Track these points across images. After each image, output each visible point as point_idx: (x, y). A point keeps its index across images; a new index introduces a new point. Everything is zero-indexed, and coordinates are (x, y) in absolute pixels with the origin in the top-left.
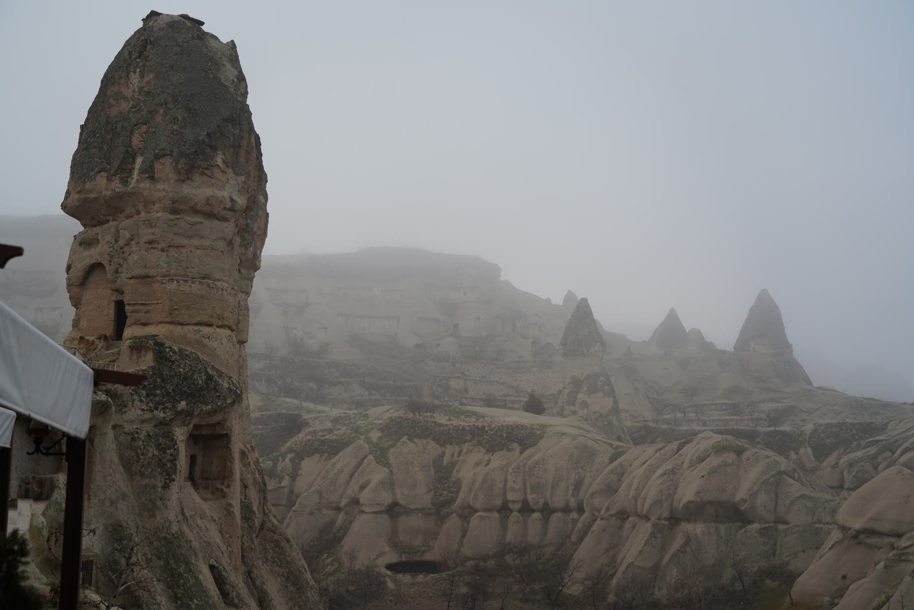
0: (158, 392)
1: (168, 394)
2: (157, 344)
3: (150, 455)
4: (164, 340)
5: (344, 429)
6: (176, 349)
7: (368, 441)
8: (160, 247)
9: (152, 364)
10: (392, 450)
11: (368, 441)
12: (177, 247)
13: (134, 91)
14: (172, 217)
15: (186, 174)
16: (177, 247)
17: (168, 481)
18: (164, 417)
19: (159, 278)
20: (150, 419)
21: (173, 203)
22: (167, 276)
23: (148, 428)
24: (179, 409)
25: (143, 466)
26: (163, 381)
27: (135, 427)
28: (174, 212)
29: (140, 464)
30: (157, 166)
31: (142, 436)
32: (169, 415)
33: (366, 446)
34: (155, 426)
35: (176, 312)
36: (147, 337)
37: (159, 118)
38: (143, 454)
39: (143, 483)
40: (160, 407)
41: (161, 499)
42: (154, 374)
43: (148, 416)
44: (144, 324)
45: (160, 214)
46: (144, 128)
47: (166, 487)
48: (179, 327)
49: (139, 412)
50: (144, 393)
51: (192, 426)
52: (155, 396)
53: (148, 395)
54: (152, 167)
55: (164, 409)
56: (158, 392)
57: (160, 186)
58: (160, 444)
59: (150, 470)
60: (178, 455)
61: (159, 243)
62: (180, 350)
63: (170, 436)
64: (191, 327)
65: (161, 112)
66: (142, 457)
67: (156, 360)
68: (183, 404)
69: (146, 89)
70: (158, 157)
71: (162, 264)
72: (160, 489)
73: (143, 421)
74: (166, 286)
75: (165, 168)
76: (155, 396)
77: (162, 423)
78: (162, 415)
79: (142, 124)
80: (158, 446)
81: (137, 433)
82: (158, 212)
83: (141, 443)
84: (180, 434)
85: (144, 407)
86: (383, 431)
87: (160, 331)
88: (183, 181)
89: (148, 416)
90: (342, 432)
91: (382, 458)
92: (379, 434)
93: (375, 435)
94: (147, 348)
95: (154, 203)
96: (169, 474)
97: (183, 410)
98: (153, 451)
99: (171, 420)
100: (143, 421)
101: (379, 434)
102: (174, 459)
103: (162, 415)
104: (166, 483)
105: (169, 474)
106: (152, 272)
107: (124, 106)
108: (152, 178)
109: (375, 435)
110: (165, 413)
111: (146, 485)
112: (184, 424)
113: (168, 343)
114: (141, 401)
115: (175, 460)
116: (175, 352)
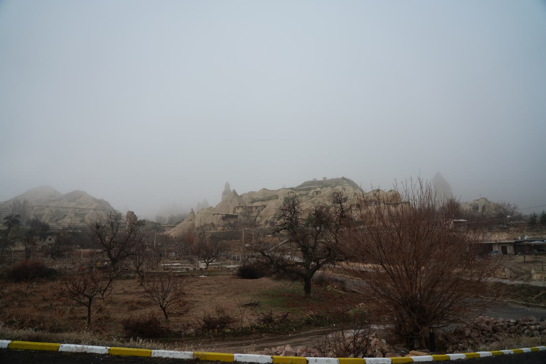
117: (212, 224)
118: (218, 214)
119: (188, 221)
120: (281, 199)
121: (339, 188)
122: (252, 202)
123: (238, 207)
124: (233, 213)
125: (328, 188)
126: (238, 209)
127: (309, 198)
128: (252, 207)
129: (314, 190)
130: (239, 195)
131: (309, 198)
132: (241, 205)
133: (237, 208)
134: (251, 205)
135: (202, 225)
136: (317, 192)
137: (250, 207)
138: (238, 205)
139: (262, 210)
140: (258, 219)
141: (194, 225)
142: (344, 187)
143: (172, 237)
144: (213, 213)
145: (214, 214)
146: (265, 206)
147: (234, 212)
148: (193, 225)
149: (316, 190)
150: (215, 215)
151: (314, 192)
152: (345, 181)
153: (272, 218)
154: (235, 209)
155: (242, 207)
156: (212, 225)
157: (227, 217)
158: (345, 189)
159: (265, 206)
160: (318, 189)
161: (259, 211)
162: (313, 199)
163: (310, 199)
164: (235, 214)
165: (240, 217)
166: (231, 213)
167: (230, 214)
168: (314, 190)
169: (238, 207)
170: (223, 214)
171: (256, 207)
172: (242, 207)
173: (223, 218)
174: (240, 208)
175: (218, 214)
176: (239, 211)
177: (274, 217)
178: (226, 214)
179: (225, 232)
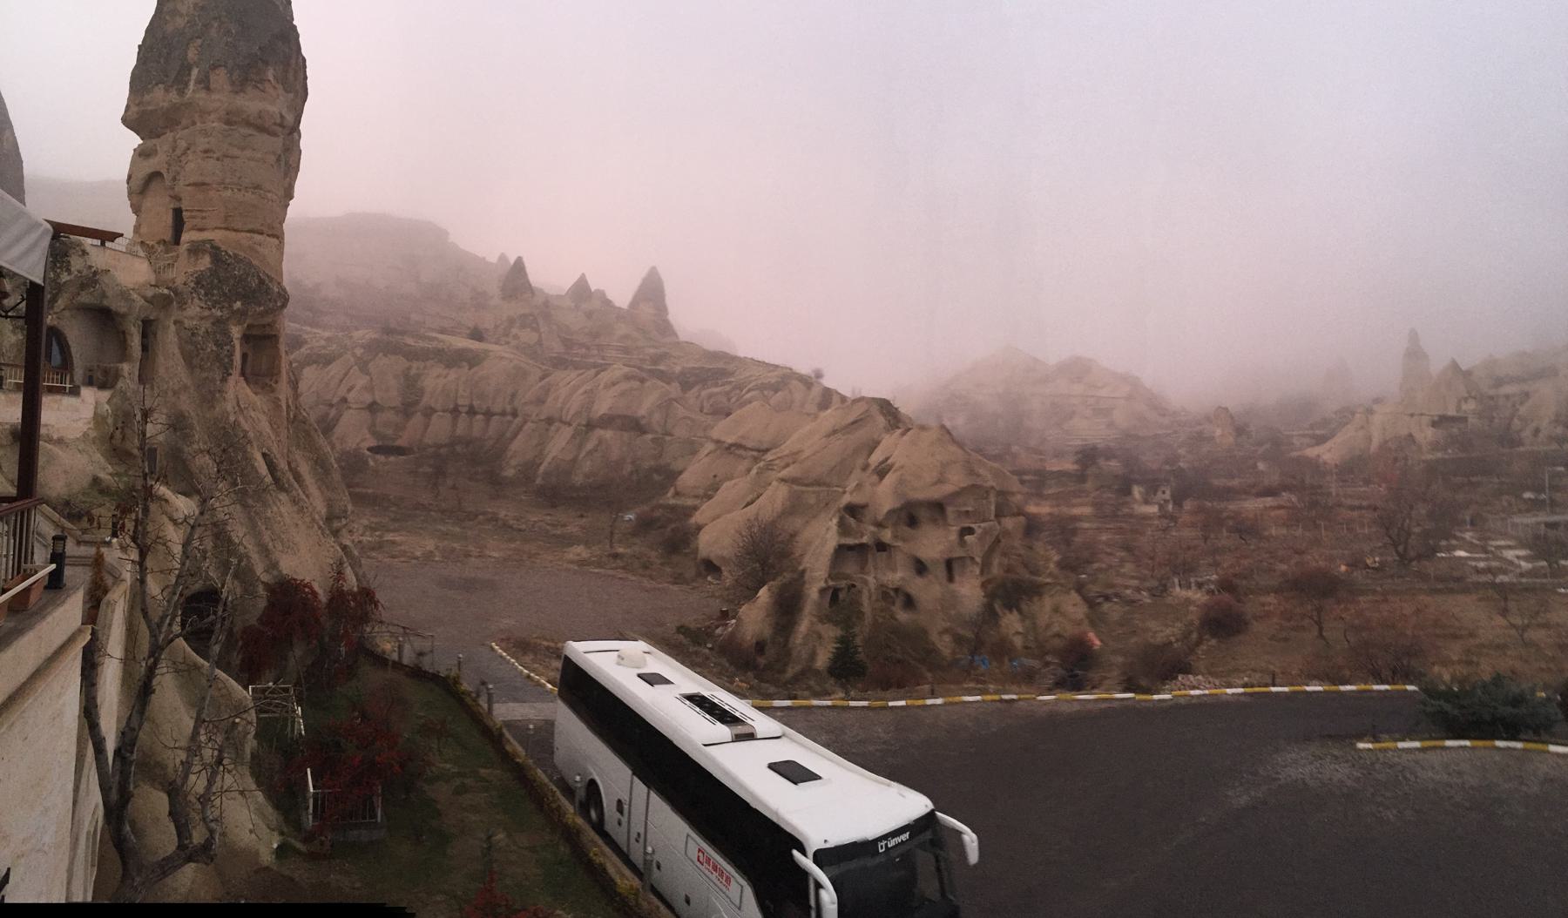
0: (215, 292)
1: (225, 294)
2: (212, 247)
3: (209, 350)
4: (220, 245)
5: (334, 347)
6: (231, 253)
7: (354, 355)
8: (215, 156)
9: (209, 266)
10: (372, 363)
11: (354, 355)
12: (232, 157)
13: (189, 8)
14: (226, 127)
15: (240, 86)
16: (232, 157)
17: (225, 375)
18: (221, 316)
19: (214, 186)
20: (209, 316)
21: (228, 114)
22: (223, 183)
23: (207, 325)
24: (235, 309)
25: (202, 359)
26: (220, 282)
27: (194, 323)
28: (228, 123)
29: (199, 358)
30: (213, 77)
31: (201, 333)
32: (226, 313)
33: (352, 359)
34: (213, 324)
35: (230, 219)
36: (204, 242)
37: (213, 32)
38: (202, 349)
39: (205, 375)
40: (218, 306)
41: (219, 391)
42: (211, 275)
43: (206, 313)
44: (201, 230)
45: (214, 125)
46: (199, 41)
47: (224, 380)
48: (234, 233)
49: (198, 309)
50: (203, 292)
51: (246, 325)
52: (213, 295)
53: (206, 294)
54: (207, 77)
55: (221, 309)
56: (215, 292)
57: (215, 96)
58: (218, 341)
59: (209, 364)
60: (234, 351)
61: (214, 153)
62: (235, 254)
63: (226, 333)
64: (243, 234)
65: (216, 25)
66: (201, 352)
67: (212, 262)
68: (238, 305)
69: (200, 5)
70: (214, 67)
71: (217, 172)
72: (218, 382)
73: (202, 318)
74: (221, 193)
75: (220, 78)
76: (213, 295)
77: (218, 322)
78: (219, 313)
79: (197, 38)
80: (217, 343)
81: (196, 329)
82: (213, 122)
83: (200, 338)
84: (236, 332)
85: (203, 305)
86: (365, 348)
87: (216, 236)
88: (237, 93)
89: (206, 313)
90: (333, 348)
91: (364, 369)
92: (362, 351)
93: (359, 352)
94: (204, 252)
95: (209, 113)
96: (226, 368)
97: (238, 309)
98: (211, 347)
99: (228, 319)
100: (202, 318)
101: (362, 351)
102: (231, 355)
103: (219, 313)
104: (223, 377)
105: (226, 368)
106: (208, 180)
107: (180, 22)
108: (208, 89)
109: (359, 352)
110: (221, 311)
111: (207, 378)
112: (239, 323)
113: (223, 248)
114: (200, 299)
115: (232, 355)
116: (230, 256)
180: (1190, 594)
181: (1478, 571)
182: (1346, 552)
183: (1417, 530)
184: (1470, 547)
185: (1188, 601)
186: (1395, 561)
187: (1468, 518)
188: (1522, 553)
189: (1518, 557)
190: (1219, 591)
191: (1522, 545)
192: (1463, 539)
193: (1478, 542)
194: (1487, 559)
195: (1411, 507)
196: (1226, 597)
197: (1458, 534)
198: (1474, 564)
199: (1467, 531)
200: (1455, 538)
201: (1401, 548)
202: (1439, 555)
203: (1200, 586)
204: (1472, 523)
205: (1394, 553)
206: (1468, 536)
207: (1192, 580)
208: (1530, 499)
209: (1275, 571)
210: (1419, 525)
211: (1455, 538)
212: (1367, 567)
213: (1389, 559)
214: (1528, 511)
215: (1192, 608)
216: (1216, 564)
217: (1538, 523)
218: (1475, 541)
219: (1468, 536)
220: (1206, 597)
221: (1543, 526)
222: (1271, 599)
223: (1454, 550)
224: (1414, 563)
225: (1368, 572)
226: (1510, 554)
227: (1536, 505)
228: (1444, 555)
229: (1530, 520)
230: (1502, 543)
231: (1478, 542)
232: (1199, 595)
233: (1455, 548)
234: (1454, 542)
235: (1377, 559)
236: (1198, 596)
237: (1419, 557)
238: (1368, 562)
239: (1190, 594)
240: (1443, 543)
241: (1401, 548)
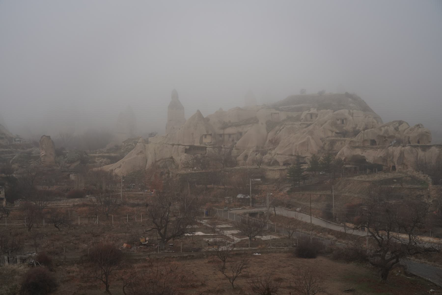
117: (172, 158)
118: (179, 145)
119: (138, 154)
120: (262, 124)
121: (345, 112)
122: (224, 128)
123: (206, 136)
124: (200, 144)
125: (328, 110)
126: (205, 137)
127: (304, 126)
128: (224, 134)
129: (307, 112)
130: (205, 117)
131: (304, 126)
132: (210, 133)
133: (204, 137)
134: (221, 132)
135: (157, 160)
136: (311, 115)
137: (221, 135)
138: (206, 133)
139: (238, 139)
140: (235, 151)
141: (147, 160)
142: (351, 111)
143: (116, 175)
144: (171, 143)
145: (173, 145)
146: (241, 134)
147: (201, 142)
148: (146, 159)
149: (310, 112)
150: (175, 146)
151: (308, 114)
152: (350, 99)
153: (253, 151)
154: (201, 138)
155: (211, 135)
156: (172, 160)
157: (190, 150)
158: (353, 113)
159: (241, 134)
160: (313, 111)
161: (233, 140)
162: (311, 127)
163: (306, 127)
164: (202, 145)
165: (209, 149)
166: (197, 144)
167: (196, 145)
168: (307, 112)
169: (206, 136)
170: (186, 144)
171: (230, 135)
172: (211, 135)
173: (186, 151)
174: (208, 137)
175: (179, 145)
176: (207, 140)
177: (256, 151)
178: (191, 144)
179: (198, 173)
180: (15, 267)
181: (209, 244)
182: (127, 234)
183: (174, 219)
184: (205, 229)
185: (14, 272)
186: (158, 239)
187: (205, 211)
188: (235, 232)
189: (233, 235)
190: (37, 264)
191: (235, 228)
192: (201, 224)
193: (210, 226)
194: (213, 237)
195: (170, 205)
196: (43, 267)
197: (198, 221)
198: (207, 240)
199: (204, 219)
200: (197, 223)
201: (162, 231)
202: (186, 235)
203: (23, 261)
204: (207, 215)
205: (159, 235)
206: (204, 222)
207: (18, 257)
208: (241, 198)
209: (78, 249)
210: (174, 216)
211: (197, 223)
212: (141, 244)
213: (155, 238)
214: (240, 206)
215: (16, 277)
216: (36, 246)
217: (245, 214)
218: (209, 226)
219: (204, 222)
220: (28, 269)
221: (247, 215)
222: (75, 268)
223: (195, 232)
224: (171, 240)
225: (141, 248)
226: (228, 233)
227: (243, 203)
228: (188, 234)
229: (240, 211)
230: (224, 226)
231: (210, 226)
232: (22, 267)
233: (195, 230)
234: (196, 226)
235: (147, 239)
236: (22, 268)
237: (174, 236)
238: (142, 240)
239: (15, 267)
240: (189, 227)
241: (162, 231)
